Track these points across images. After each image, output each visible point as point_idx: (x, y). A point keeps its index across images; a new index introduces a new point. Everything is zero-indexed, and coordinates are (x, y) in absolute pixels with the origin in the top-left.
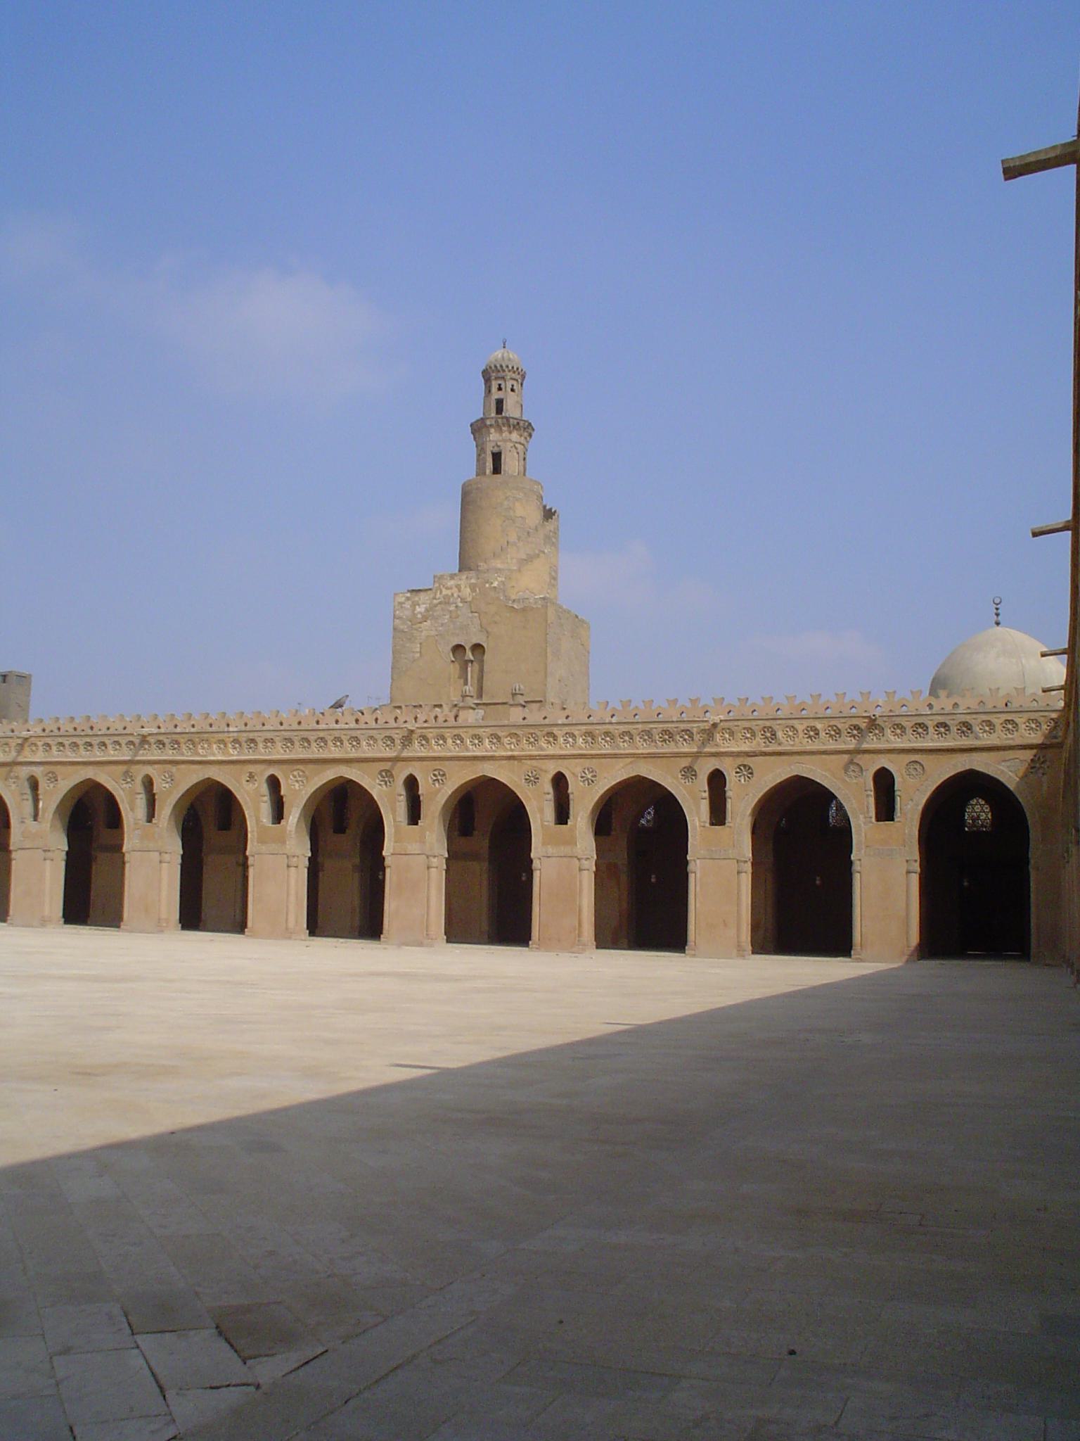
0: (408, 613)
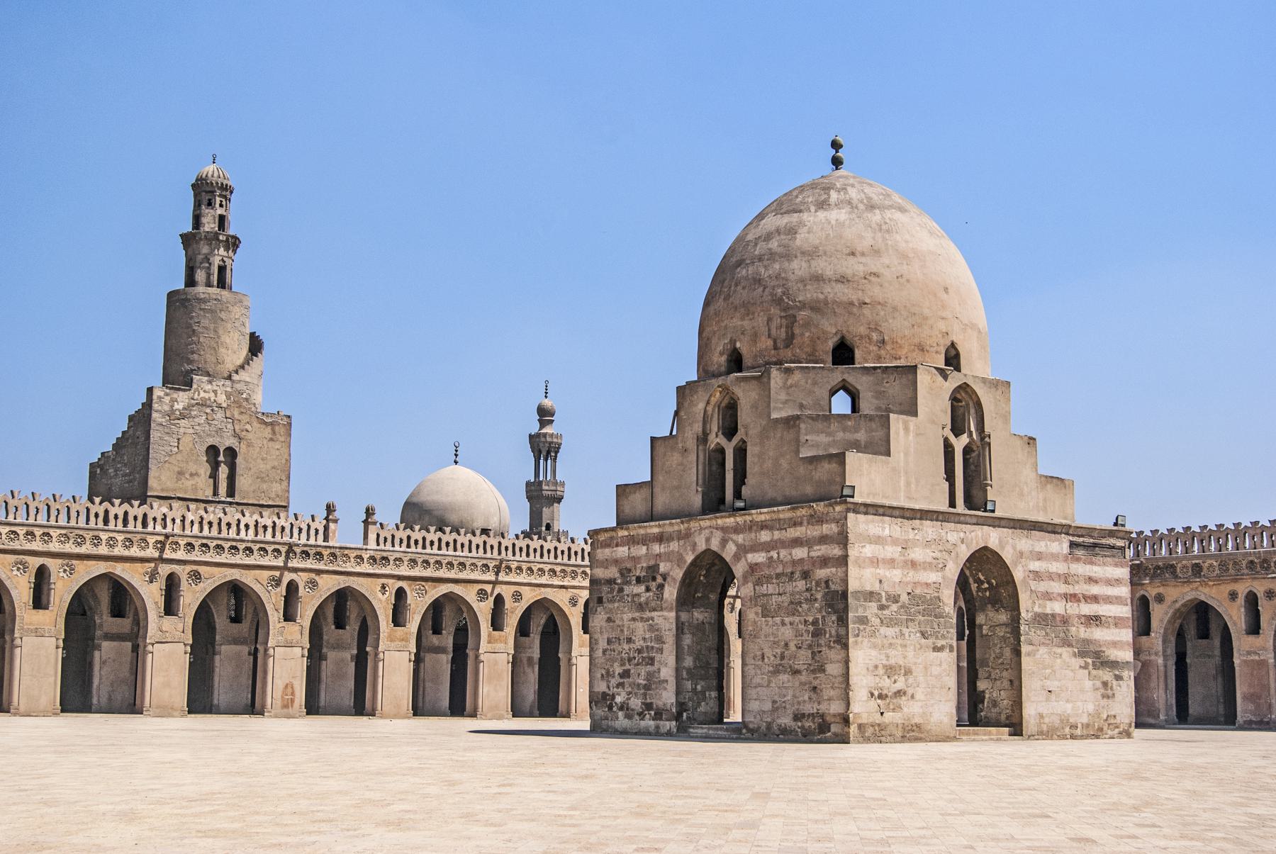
0: (167, 408)
